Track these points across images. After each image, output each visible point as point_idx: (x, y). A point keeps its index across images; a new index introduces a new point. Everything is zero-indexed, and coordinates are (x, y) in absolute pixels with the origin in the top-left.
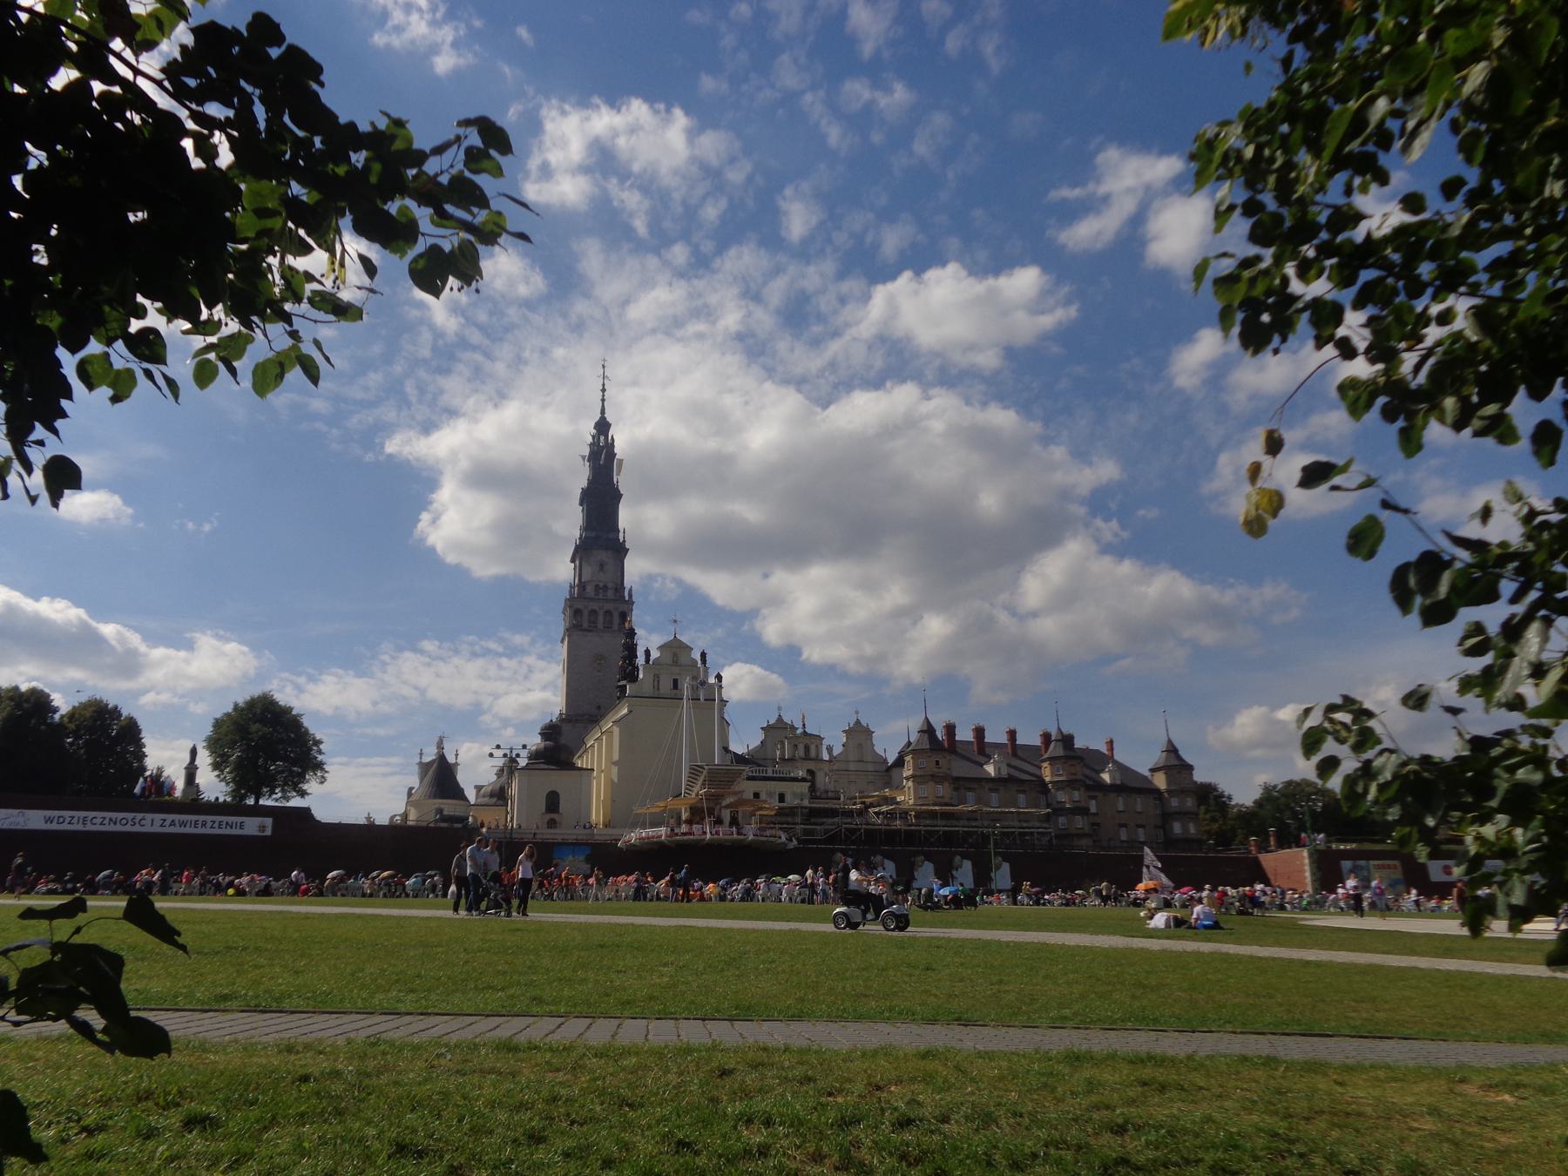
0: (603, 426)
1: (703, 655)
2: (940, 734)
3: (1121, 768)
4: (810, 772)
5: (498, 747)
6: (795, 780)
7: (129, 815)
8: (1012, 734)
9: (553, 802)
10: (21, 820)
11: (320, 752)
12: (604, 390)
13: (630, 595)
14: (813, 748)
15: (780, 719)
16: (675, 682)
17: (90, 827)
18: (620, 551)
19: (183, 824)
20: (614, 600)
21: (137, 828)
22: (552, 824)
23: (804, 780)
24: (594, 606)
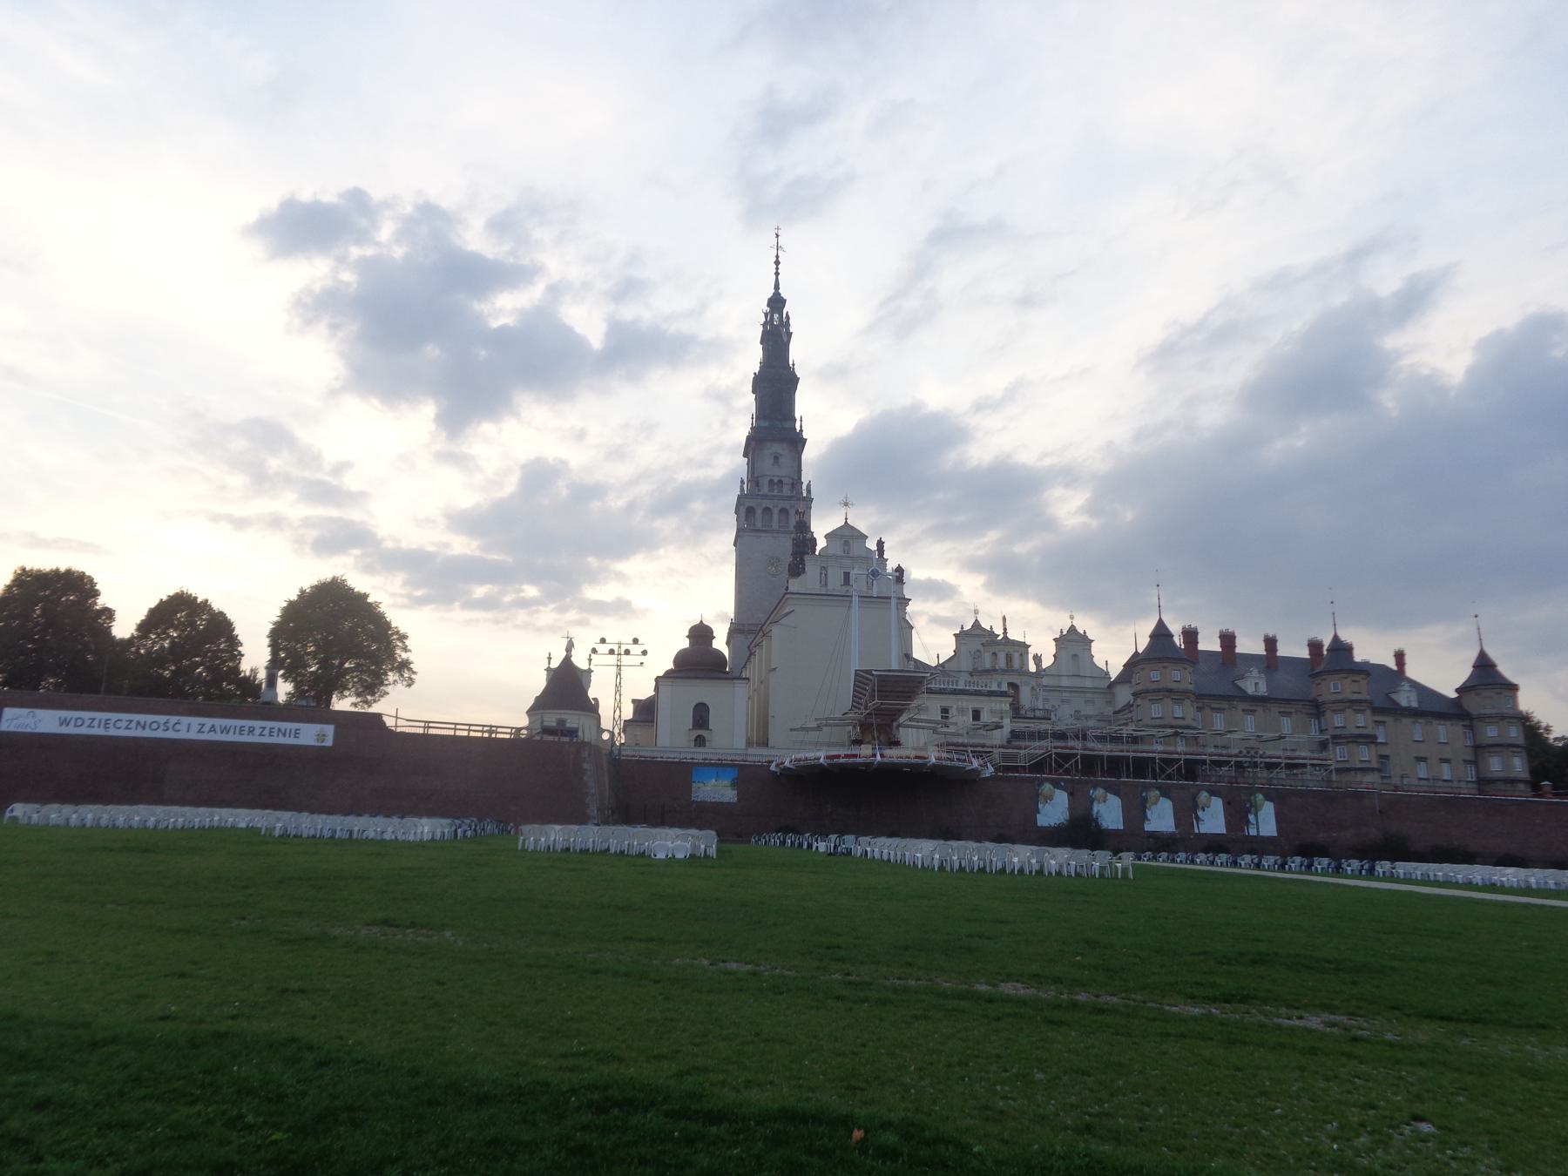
1: (880, 544)
2: (1178, 640)
3: (1416, 686)
4: (1012, 685)
5: (603, 641)
6: (991, 694)
7: (162, 719)
8: (1271, 643)
9: (701, 716)
10: (31, 721)
11: (405, 649)
12: (777, 263)
13: (809, 491)
14: (1016, 656)
15: (977, 624)
16: (847, 575)
17: (112, 732)
18: (798, 442)
20: (790, 498)
22: (700, 741)
23: (1003, 694)
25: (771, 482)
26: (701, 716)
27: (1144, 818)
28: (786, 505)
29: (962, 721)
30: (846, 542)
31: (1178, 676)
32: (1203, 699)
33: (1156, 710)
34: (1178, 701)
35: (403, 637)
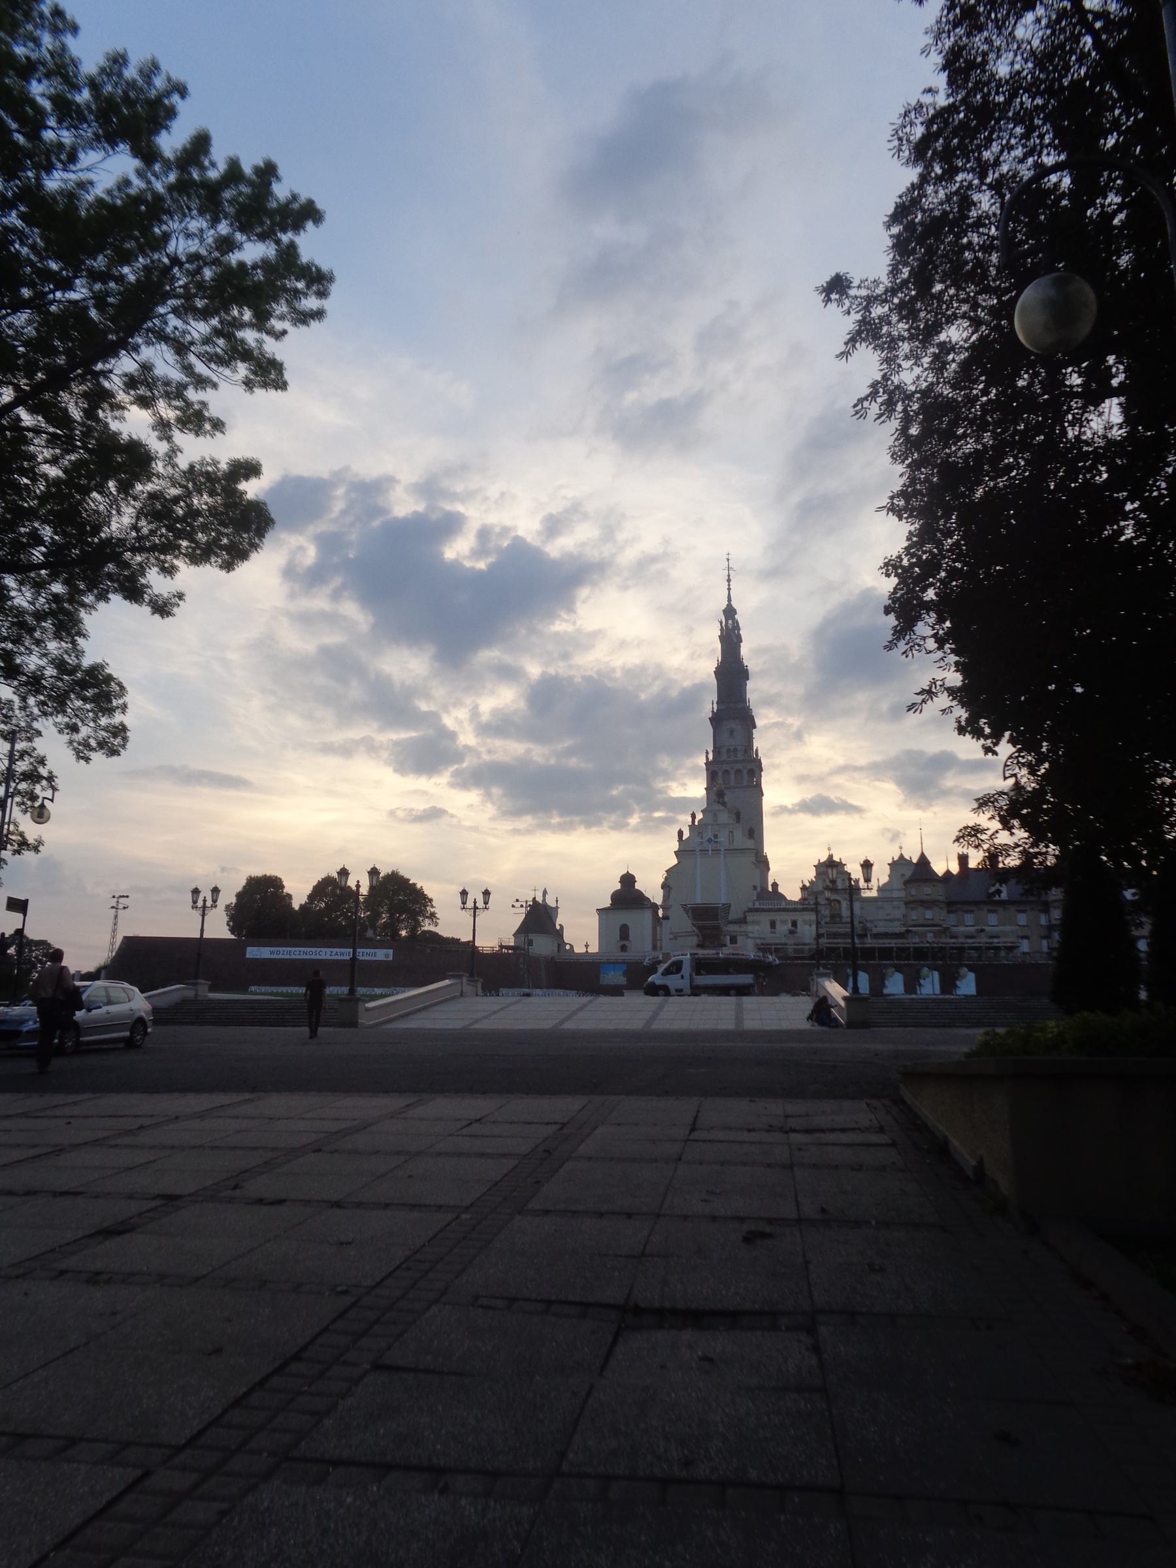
0: (730, 612)
9: (624, 932)
11: (432, 907)
12: (729, 580)
15: (831, 856)
17: (293, 957)
19: (342, 954)
21: (318, 957)
24: (725, 767)
25: (728, 750)
26: (624, 932)
27: (883, 985)
28: (739, 766)
29: (783, 928)
30: (715, 815)
31: (927, 890)
32: (951, 905)
33: (914, 915)
34: (928, 908)
35: (431, 900)
